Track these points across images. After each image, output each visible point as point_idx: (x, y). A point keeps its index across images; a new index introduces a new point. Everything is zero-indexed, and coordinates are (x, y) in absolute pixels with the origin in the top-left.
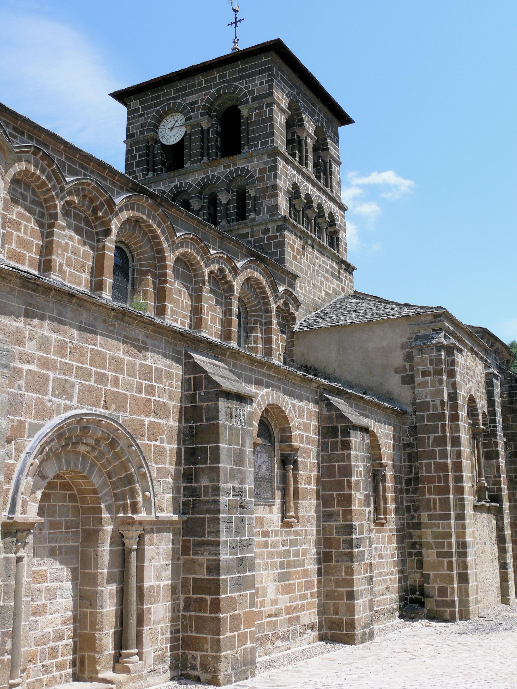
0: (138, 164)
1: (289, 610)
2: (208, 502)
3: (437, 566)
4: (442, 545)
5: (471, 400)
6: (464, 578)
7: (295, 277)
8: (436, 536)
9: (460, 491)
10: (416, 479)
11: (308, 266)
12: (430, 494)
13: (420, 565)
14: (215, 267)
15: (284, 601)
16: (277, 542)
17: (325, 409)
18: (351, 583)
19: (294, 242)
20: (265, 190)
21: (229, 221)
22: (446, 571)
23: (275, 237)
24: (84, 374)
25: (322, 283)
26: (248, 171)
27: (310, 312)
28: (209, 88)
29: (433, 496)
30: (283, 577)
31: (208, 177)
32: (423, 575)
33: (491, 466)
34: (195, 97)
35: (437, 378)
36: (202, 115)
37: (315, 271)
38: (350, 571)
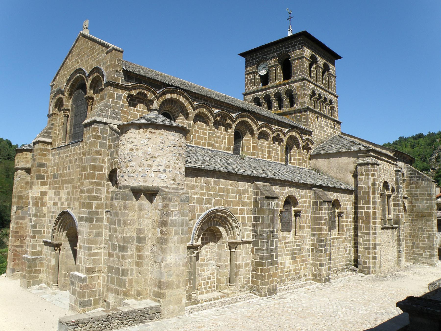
0: (250, 83)
1: (295, 270)
2: (260, 235)
3: (363, 253)
4: (366, 244)
6: (375, 258)
7: (311, 132)
9: (375, 223)
11: (319, 126)
12: (362, 224)
14: (275, 134)
15: (293, 267)
16: (291, 245)
17: (313, 194)
19: (312, 116)
20: (300, 95)
22: (367, 255)
23: (304, 115)
24: (216, 196)
25: (325, 131)
26: (293, 87)
27: (319, 145)
28: (278, 51)
29: (363, 225)
30: (293, 258)
31: (277, 89)
35: (366, 177)
37: (322, 127)
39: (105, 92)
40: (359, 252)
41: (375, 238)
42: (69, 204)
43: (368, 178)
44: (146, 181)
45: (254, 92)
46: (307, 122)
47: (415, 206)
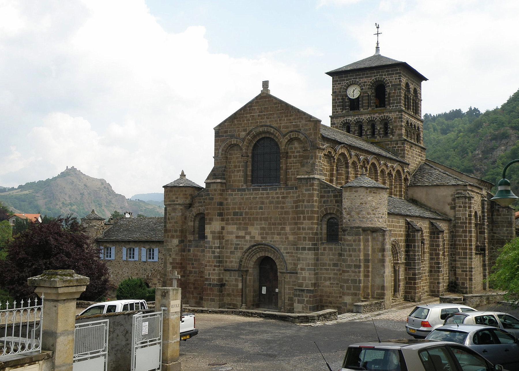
0: (338, 106)
4: (463, 268)
5: (476, 212)
6: (471, 280)
8: (461, 264)
10: (455, 245)
13: (455, 274)
18: (439, 279)
20: (397, 126)
21: (380, 137)
23: (401, 147)
26: (390, 118)
28: (372, 77)
31: (371, 117)
32: (456, 278)
33: (482, 237)
34: (365, 80)
36: (368, 88)
38: (438, 276)
39: (310, 153)
40: (457, 274)
41: (472, 262)
42: (262, 238)
43: (466, 210)
44: (372, 224)
45: (344, 117)
46: (404, 153)
47: (495, 233)
